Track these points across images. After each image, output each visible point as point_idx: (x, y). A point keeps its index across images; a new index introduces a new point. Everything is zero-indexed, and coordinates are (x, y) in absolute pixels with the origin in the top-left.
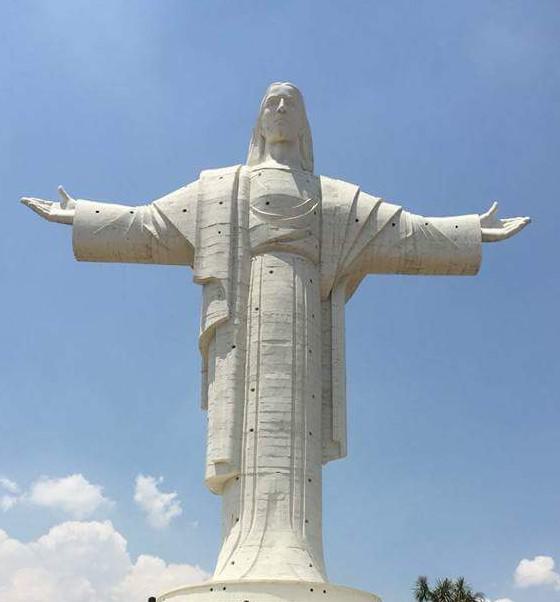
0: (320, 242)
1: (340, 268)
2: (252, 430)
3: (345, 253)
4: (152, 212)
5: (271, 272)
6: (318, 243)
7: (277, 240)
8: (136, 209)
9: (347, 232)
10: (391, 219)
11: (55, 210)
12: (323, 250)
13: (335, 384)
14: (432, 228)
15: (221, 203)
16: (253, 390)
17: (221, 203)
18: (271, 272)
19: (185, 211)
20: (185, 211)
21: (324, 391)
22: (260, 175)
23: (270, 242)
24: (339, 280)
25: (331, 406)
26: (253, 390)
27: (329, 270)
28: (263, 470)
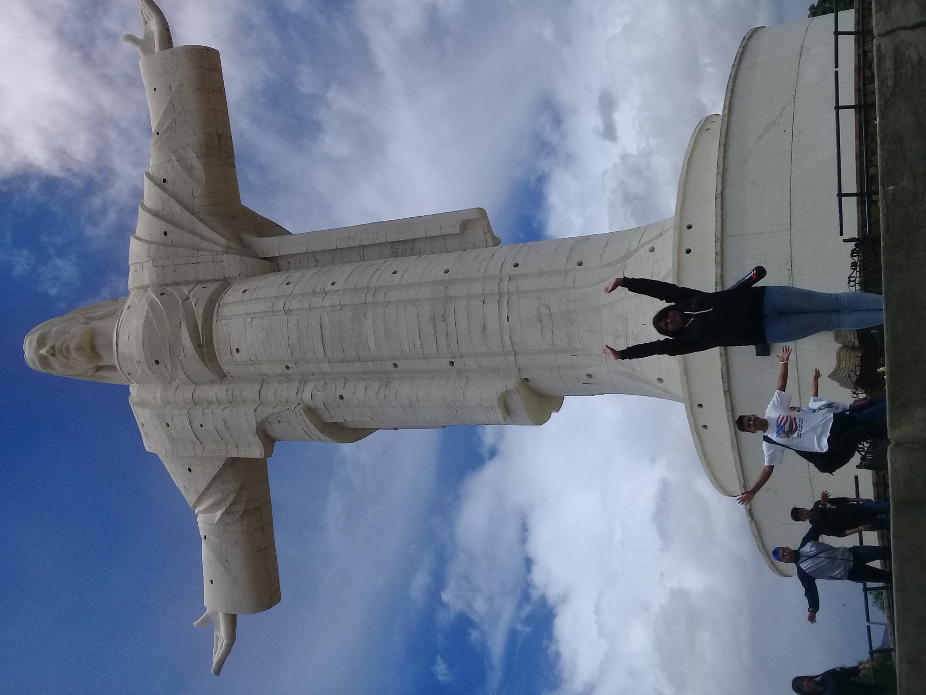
0: (199, 282)
1: (227, 250)
2: (452, 363)
3: (211, 245)
4: (205, 511)
5: (238, 351)
6: (200, 286)
7: (198, 346)
8: (202, 534)
9: (182, 246)
10: (158, 185)
11: (221, 633)
12: (208, 278)
13: (382, 239)
14: (161, 123)
15: (168, 425)
16: (395, 365)
17: (168, 425)
18: (238, 351)
19: (190, 470)
20: (190, 470)
21: (396, 255)
22: (129, 374)
23: (202, 356)
24: (245, 250)
25: (414, 240)
26: (395, 365)
27: (231, 264)
28: (507, 342)
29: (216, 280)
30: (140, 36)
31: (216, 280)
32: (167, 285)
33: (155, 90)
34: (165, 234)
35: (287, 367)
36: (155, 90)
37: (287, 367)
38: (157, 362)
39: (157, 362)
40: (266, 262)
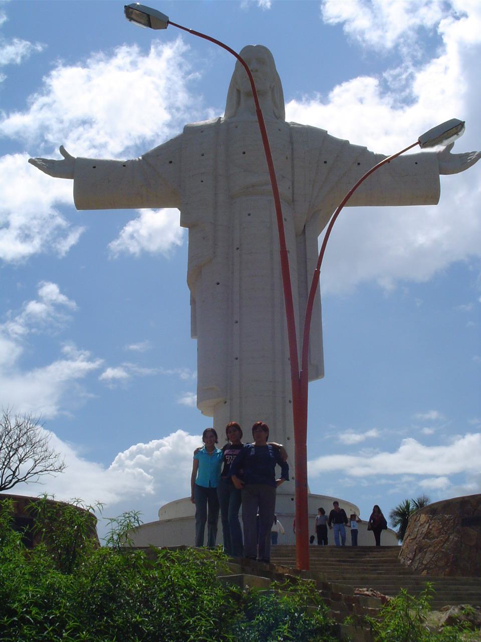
2: (237, 359)
18: (249, 215)
19: (171, 162)
20: (171, 162)
29: (293, 194)
30: (453, 151)
31: (293, 194)
32: (293, 160)
33: (416, 163)
34: (325, 162)
35: (238, 249)
36: (416, 163)
37: (238, 249)
38: (244, 153)
39: (244, 153)
40: (303, 227)
